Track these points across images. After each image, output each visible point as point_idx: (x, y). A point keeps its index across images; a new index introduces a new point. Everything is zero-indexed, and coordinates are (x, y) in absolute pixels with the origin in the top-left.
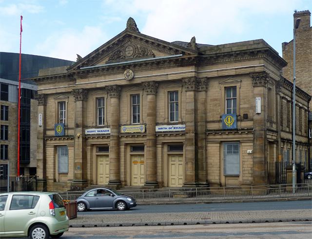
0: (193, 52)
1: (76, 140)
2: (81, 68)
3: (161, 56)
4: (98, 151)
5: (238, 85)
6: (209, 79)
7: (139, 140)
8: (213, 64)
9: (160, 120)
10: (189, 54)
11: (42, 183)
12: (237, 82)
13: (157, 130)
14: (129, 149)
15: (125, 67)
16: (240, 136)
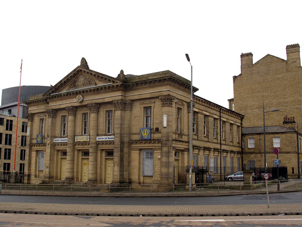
0: (119, 81)
3: (100, 84)
4: (107, 155)
5: (152, 105)
7: (86, 147)
8: (135, 90)
10: (117, 82)
11: (27, 177)
12: (151, 103)
13: (97, 140)
14: (80, 154)
15: (77, 93)
16: (153, 145)
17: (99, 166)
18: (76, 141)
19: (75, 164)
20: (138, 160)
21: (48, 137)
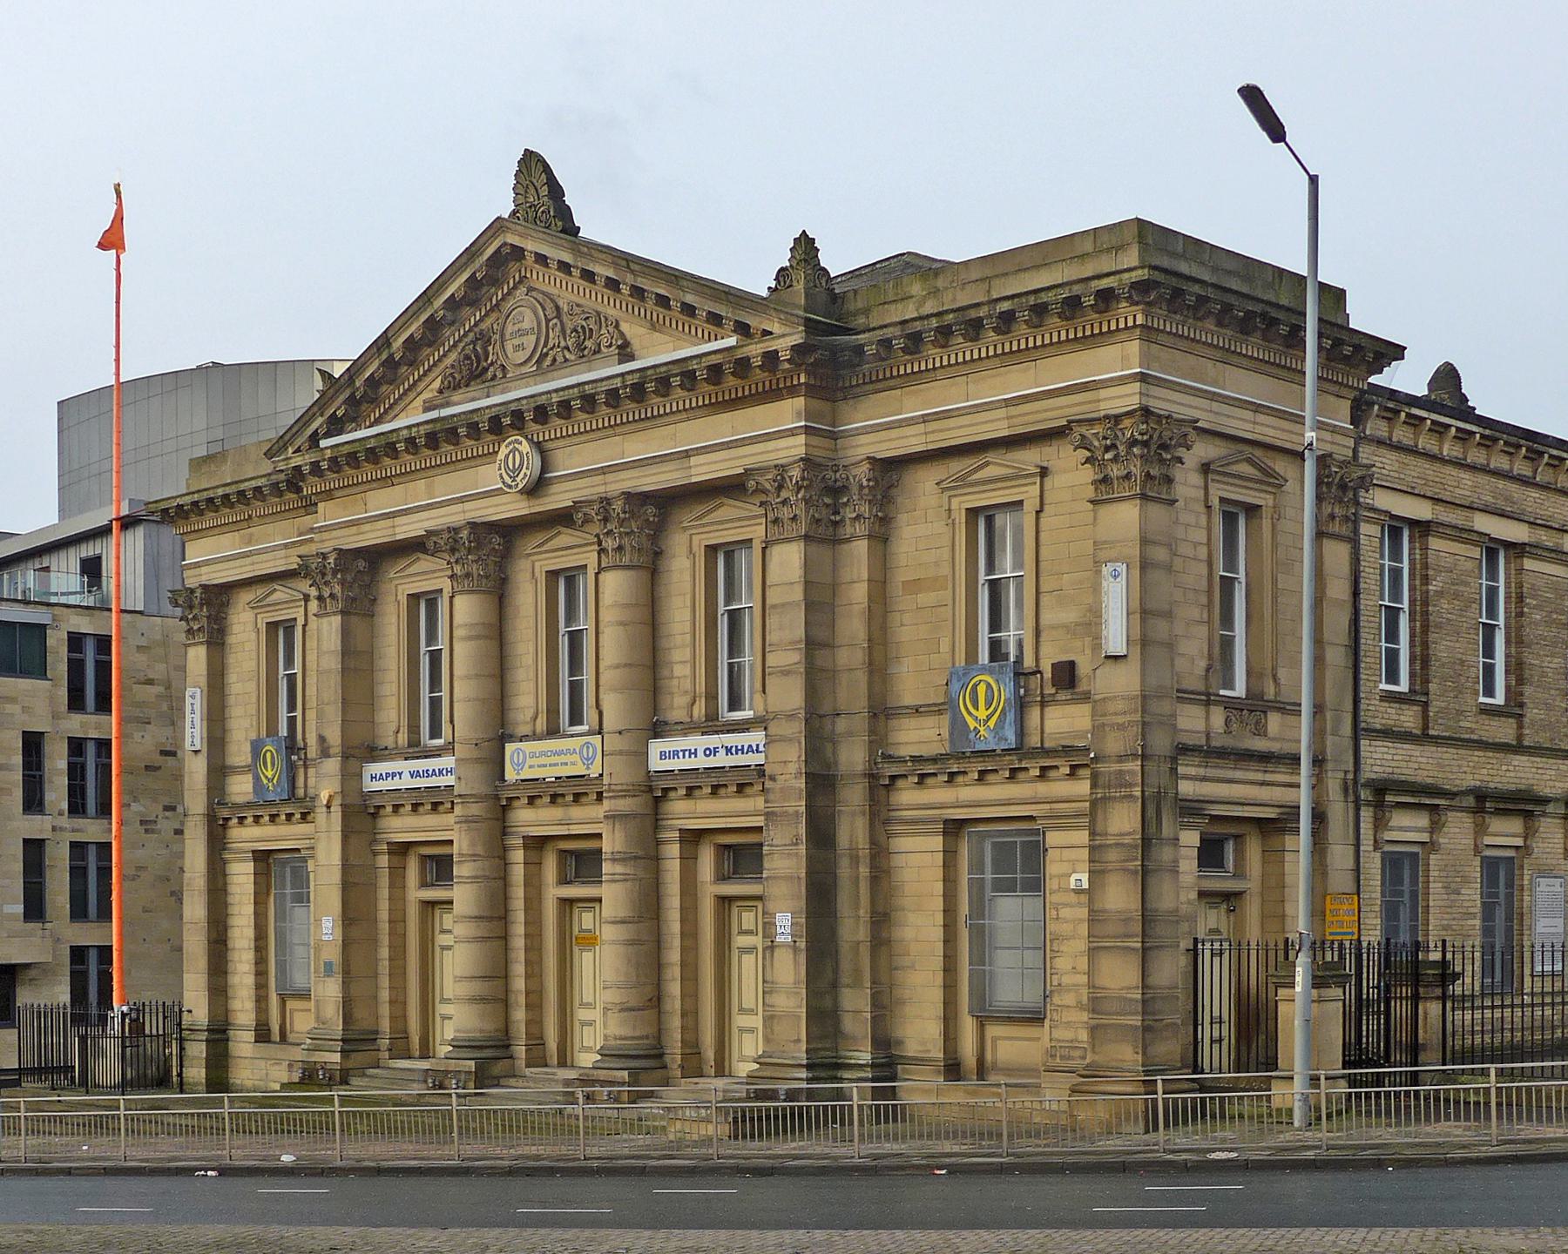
1: (320, 814)
2: (323, 443)
6: (891, 468)
7: (584, 818)
9: (676, 707)
10: (766, 333)
11: (203, 1046)
13: (656, 764)
15: (498, 425)
16: (1042, 789)
17: (674, 955)
18: (511, 775)
19: (518, 942)
20: (939, 903)
21: (325, 753)
